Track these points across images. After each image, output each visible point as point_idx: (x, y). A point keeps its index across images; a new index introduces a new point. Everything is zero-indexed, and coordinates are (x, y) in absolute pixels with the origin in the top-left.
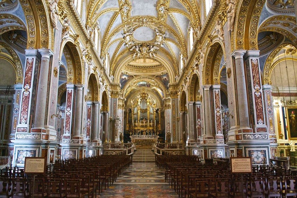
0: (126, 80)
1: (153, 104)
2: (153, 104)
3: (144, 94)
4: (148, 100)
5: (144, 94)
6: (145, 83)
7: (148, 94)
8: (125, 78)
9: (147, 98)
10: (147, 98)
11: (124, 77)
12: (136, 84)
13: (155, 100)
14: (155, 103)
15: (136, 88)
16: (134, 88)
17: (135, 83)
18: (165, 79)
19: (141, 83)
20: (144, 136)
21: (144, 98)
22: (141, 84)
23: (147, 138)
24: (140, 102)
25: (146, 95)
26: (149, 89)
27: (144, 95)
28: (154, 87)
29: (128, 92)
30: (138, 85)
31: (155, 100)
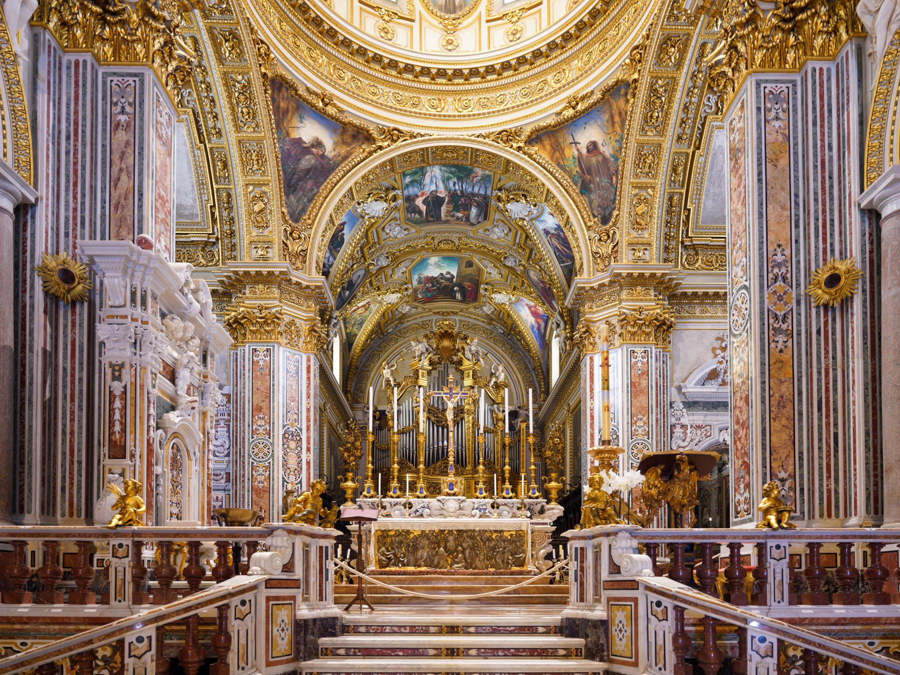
0: (323, 156)
1: (492, 383)
2: (492, 383)
3: (446, 335)
4: (466, 363)
5: (446, 335)
6: (455, 273)
7: (466, 338)
8: (318, 144)
9: (464, 354)
10: (464, 354)
11: (308, 131)
12: (402, 268)
13: (501, 368)
14: (502, 377)
15: (406, 309)
16: (393, 298)
17: (395, 259)
18: (593, 147)
19: (435, 268)
20: (452, 503)
21: (446, 361)
22: (431, 280)
23: (472, 521)
24: (429, 373)
25: (459, 344)
26: (472, 314)
27: (446, 343)
28: (501, 298)
29: (368, 327)
30: (415, 277)
31: (501, 368)
